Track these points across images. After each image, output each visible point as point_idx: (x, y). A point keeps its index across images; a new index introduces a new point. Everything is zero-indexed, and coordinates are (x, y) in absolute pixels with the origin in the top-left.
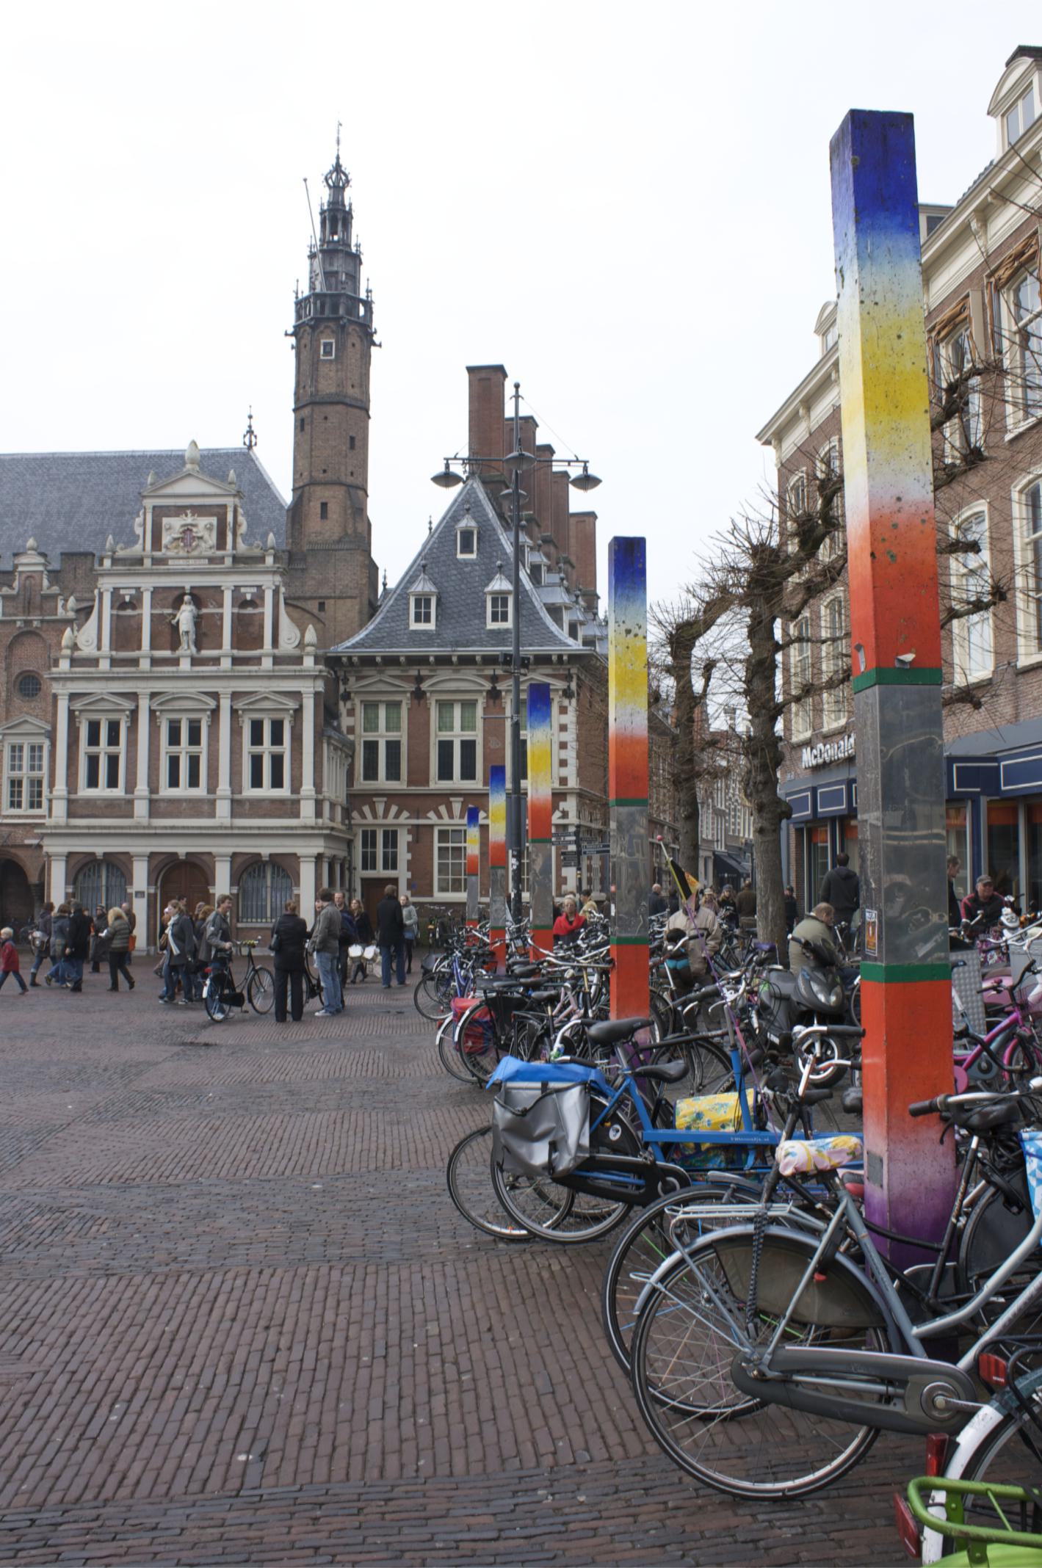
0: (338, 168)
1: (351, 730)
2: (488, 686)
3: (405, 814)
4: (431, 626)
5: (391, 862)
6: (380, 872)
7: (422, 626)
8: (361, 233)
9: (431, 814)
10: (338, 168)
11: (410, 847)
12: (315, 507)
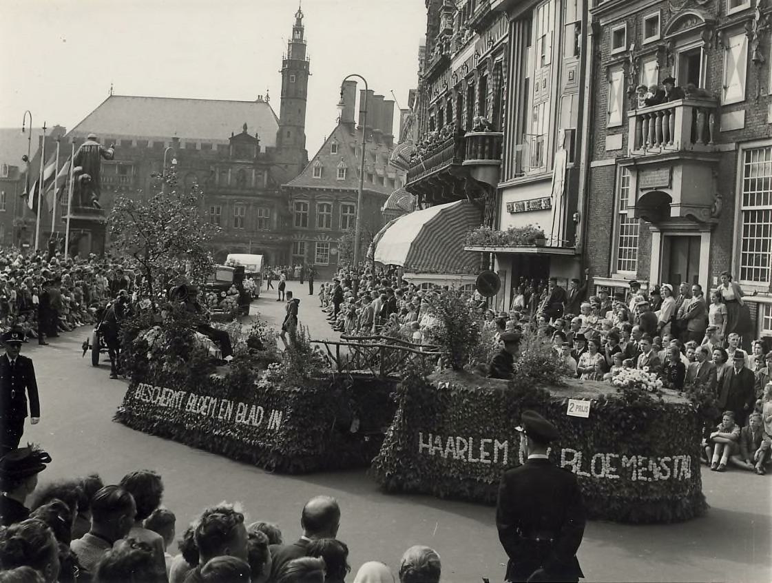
0: (300, 11)
1: (292, 210)
2: (335, 199)
3: (307, 237)
4: (320, 177)
5: (302, 252)
6: (299, 255)
7: (317, 177)
8: (307, 36)
9: (315, 238)
10: (300, 11)
11: (309, 248)
12: (285, 134)
